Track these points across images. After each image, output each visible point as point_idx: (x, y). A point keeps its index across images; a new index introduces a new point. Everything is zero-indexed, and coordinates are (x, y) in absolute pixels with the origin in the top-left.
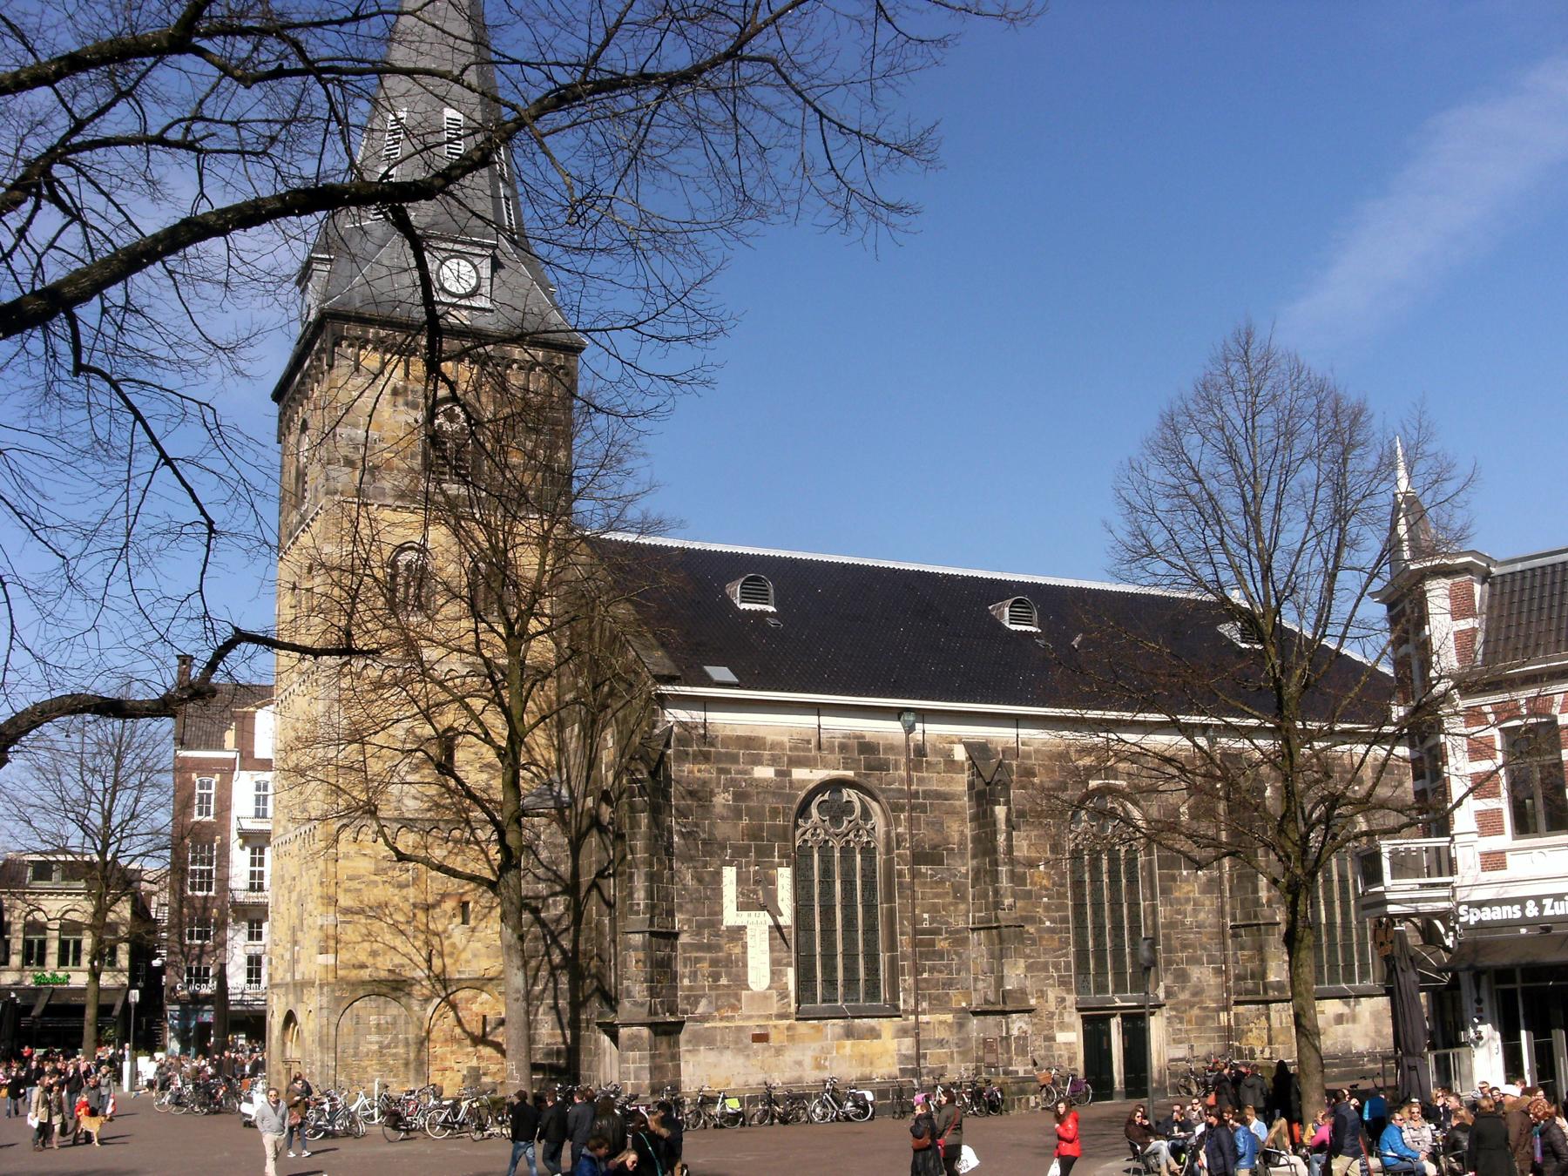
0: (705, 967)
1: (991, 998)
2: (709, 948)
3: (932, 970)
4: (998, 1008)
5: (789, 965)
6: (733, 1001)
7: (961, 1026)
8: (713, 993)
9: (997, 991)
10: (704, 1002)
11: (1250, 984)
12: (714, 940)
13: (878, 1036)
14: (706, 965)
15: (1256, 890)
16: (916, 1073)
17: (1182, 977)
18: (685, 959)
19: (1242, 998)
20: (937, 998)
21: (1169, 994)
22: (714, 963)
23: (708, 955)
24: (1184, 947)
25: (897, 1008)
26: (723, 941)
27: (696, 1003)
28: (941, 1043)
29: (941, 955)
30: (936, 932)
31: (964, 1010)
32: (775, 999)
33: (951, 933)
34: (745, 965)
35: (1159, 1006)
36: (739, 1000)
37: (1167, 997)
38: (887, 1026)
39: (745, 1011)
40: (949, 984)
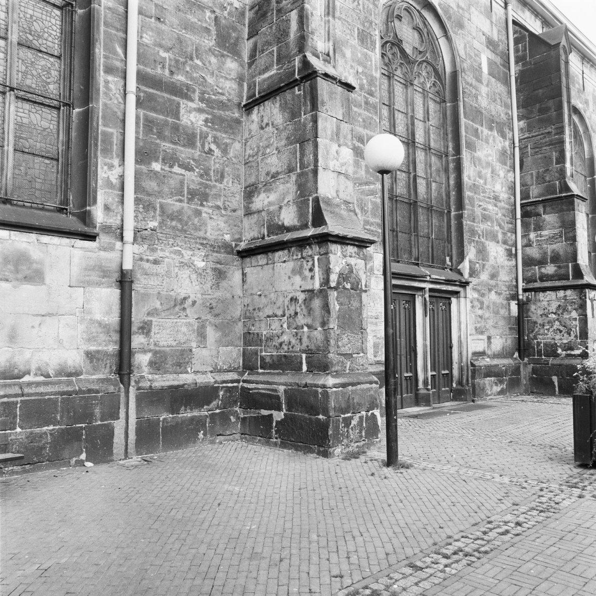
1: (289, 217)
3: (171, 160)
4: (310, 232)
7: (220, 275)
9: (301, 205)
11: (550, 269)
13: (35, 276)
15: (561, 159)
16: (123, 364)
17: (482, 252)
19: (538, 285)
20: (176, 216)
21: (473, 273)
24: (486, 218)
25: (85, 217)
28: (179, 304)
29: (190, 140)
30: (182, 92)
31: (227, 248)
33: (209, 102)
35: (464, 284)
37: (471, 275)
38: (62, 255)
40: (200, 195)
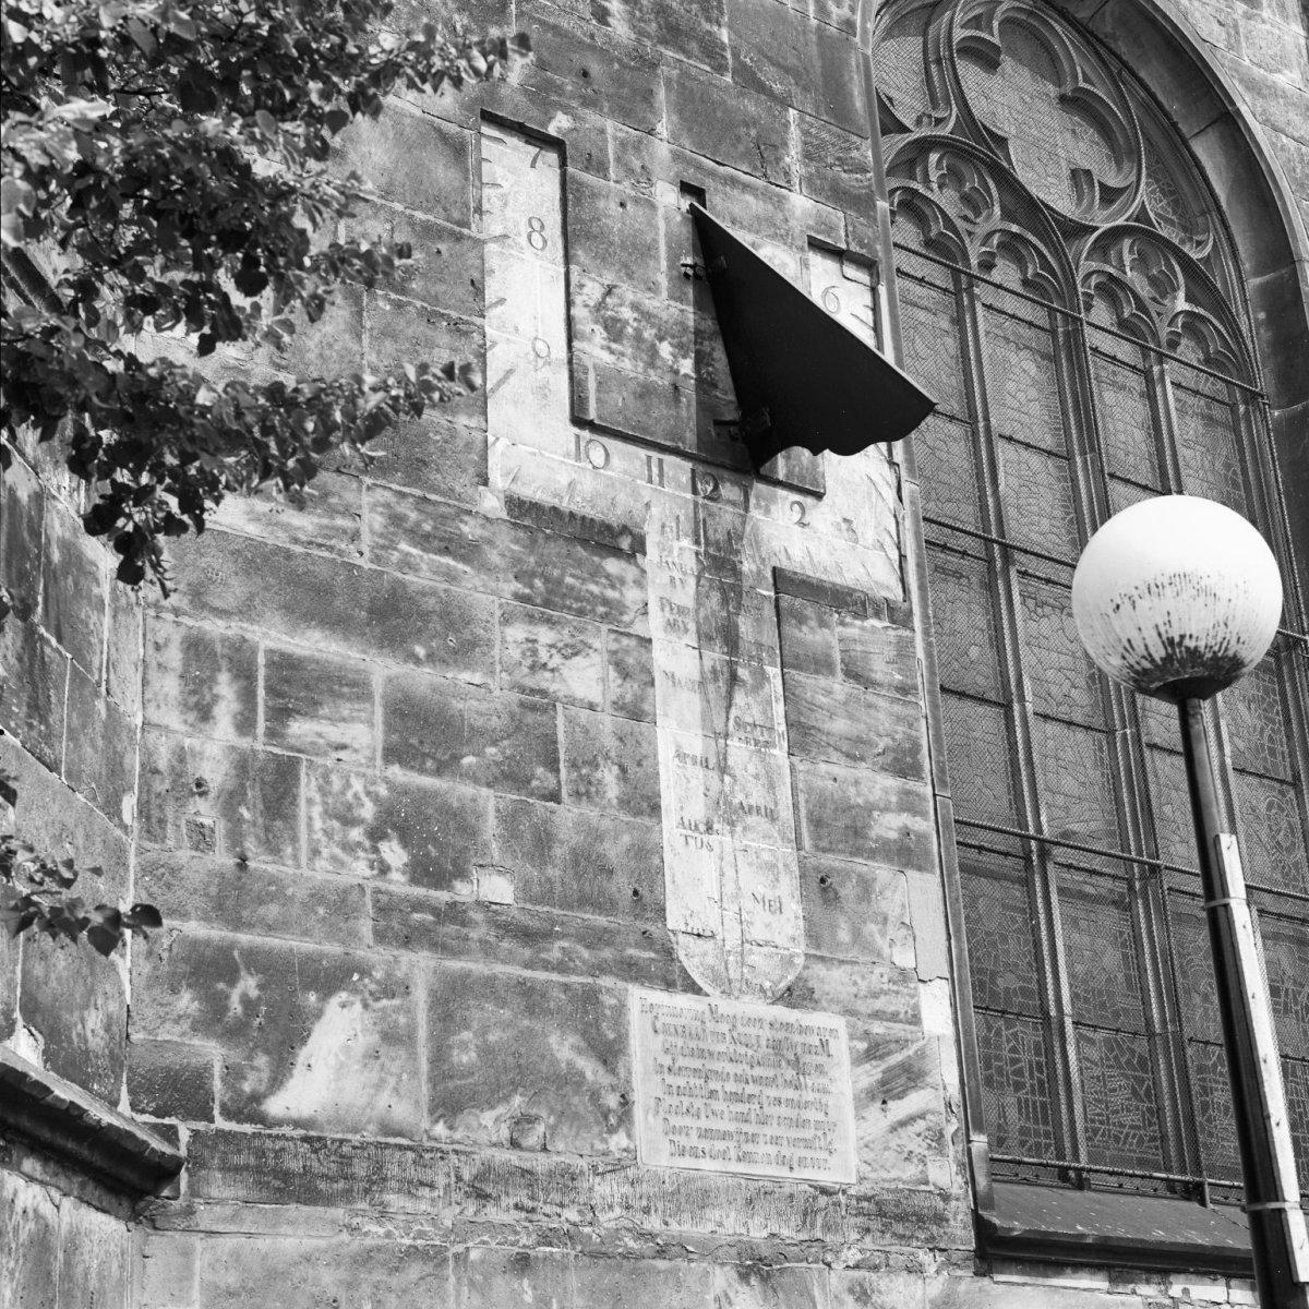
0: (348, 747)
2: (391, 617)
5: (905, 854)
6: (564, 1048)
8: (420, 966)
10: (338, 1030)
12: (424, 571)
14: (363, 733)
18: (196, 647)
22: (420, 732)
23: (382, 669)
26: (485, 593)
27: (281, 1036)
32: (846, 1079)
34: (642, 801)
36: (609, 1053)
39: (652, 1143)
